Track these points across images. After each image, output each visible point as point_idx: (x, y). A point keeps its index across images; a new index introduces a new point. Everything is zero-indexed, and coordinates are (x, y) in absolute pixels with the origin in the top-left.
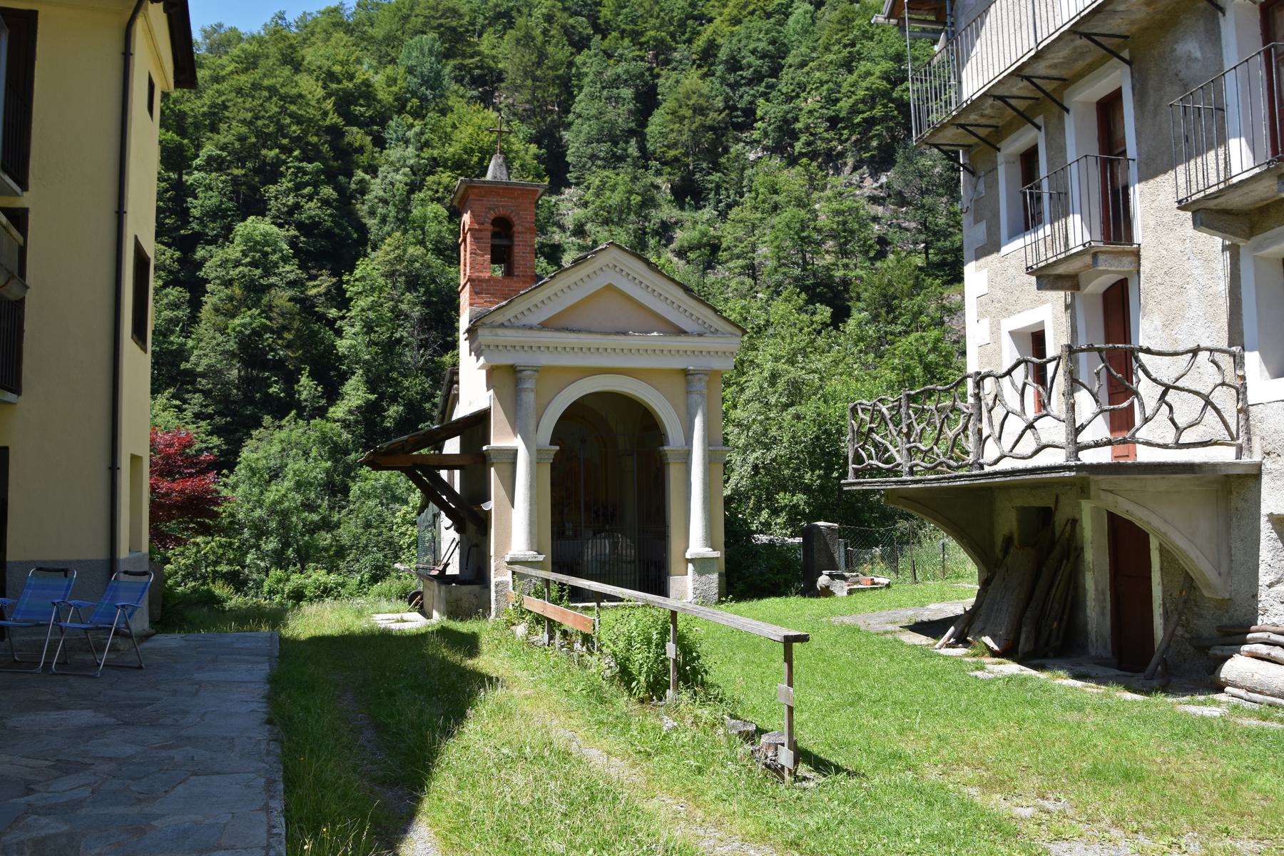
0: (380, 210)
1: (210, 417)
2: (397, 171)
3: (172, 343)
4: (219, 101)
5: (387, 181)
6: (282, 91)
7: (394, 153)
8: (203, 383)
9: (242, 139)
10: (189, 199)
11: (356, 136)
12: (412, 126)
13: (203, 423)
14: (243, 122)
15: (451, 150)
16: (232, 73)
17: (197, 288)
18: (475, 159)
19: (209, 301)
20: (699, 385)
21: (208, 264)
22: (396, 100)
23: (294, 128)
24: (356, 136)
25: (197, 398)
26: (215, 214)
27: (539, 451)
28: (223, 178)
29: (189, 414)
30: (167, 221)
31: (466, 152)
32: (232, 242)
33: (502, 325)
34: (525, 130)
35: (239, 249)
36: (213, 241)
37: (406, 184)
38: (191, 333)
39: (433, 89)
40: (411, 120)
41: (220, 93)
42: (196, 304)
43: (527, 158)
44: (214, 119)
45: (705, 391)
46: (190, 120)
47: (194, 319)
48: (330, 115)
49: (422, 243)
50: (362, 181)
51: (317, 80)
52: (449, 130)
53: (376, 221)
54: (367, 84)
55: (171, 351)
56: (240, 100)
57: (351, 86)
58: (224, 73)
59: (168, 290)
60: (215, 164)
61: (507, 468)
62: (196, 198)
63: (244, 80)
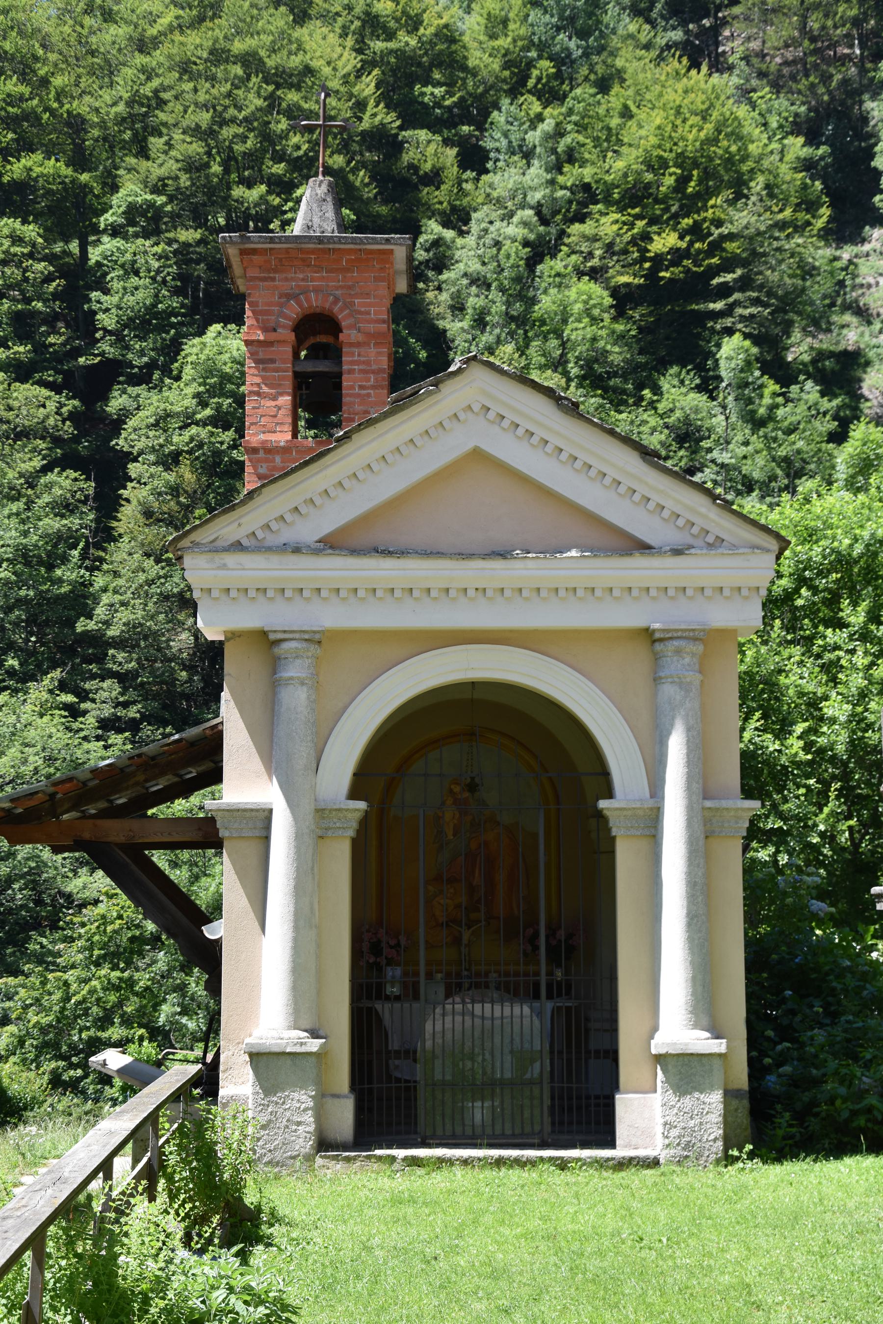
0: (471, 302)
1: (133, 726)
2: (508, 216)
3: (60, 581)
4: (147, 90)
5: (488, 240)
6: (270, 63)
7: (503, 179)
8: (120, 660)
9: (192, 166)
10: (95, 295)
11: (426, 148)
12: (540, 118)
13: (115, 739)
14: (196, 132)
15: (620, 164)
16: (171, 29)
17: (108, 472)
18: (669, 181)
19: (135, 496)
20: (680, 663)
21: (131, 423)
22: (506, 66)
23: (295, 139)
24: (426, 148)
25: (109, 689)
26: (145, 322)
27: (321, 812)
28: (158, 249)
29: (90, 720)
30: (52, 339)
31: (650, 168)
32: (178, 378)
33: (238, 547)
34: (784, 107)
35: (190, 390)
36: (143, 378)
37: (526, 243)
38: (102, 560)
39: (583, 34)
40: (536, 107)
41: (149, 74)
42: (107, 503)
43: (784, 168)
44: (139, 130)
45: (694, 678)
46: (96, 133)
47: (104, 534)
48: (370, 109)
49: (558, 365)
50: (438, 242)
51: (344, 35)
52: (615, 122)
53: (466, 324)
54: (448, 36)
55: (59, 598)
56: (188, 86)
57: (413, 42)
58: (153, 31)
59: (51, 477)
60: (145, 221)
61: (251, 849)
62: (106, 292)
63: (196, 42)
